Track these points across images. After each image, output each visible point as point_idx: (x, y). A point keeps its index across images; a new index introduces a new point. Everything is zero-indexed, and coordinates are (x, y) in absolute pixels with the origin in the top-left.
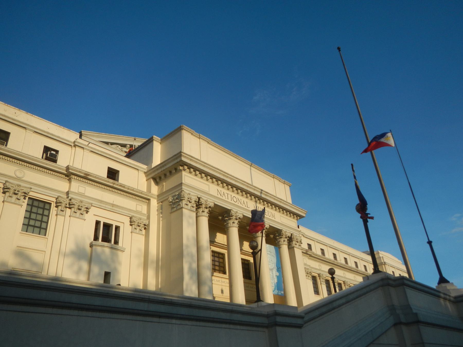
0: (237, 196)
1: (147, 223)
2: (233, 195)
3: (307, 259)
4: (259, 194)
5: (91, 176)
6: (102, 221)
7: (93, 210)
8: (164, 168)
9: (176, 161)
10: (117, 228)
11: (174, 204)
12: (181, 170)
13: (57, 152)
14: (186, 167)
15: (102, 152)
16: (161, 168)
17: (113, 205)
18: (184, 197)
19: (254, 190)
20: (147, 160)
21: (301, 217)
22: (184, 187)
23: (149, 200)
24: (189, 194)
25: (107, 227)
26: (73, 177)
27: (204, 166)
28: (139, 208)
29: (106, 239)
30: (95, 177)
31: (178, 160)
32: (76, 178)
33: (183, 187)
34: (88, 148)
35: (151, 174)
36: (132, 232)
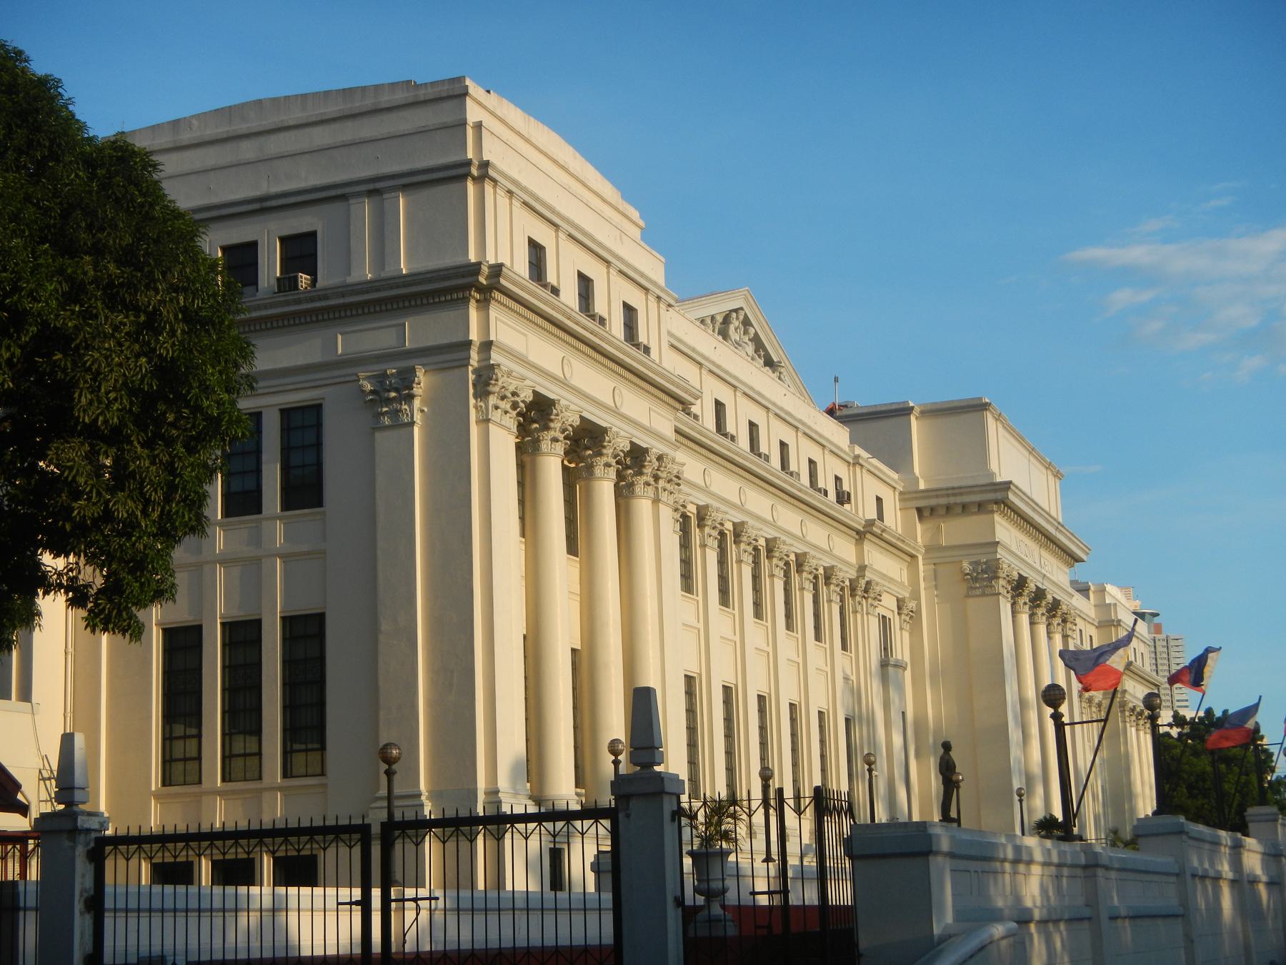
1: (912, 605)
4: (1052, 530)
8: (959, 500)
9: (992, 496)
11: (975, 580)
12: (992, 512)
15: (876, 467)
16: (948, 495)
17: (891, 580)
20: (897, 456)
21: (1077, 560)
22: (1001, 553)
23: (913, 557)
31: (999, 496)
33: (999, 550)
35: (916, 498)
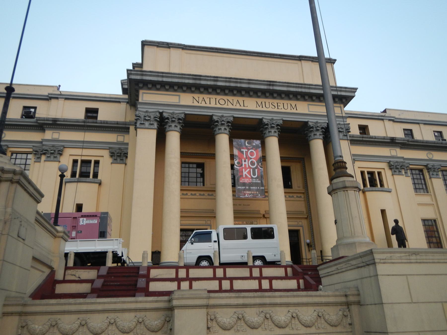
0: (226, 98)
2: (219, 97)
3: (398, 150)
5: (59, 121)
6: (79, 159)
7: (68, 152)
10: (97, 163)
13: (35, 108)
14: (141, 85)
18: (139, 117)
19: (249, 83)
24: (147, 112)
25: (86, 163)
26: (45, 126)
27: (163, 77)
28: (121, 139)
29: (84, 175)
30: (64, 121)
32: (47, 126)
34: (62, 96)
36: (112, 163)
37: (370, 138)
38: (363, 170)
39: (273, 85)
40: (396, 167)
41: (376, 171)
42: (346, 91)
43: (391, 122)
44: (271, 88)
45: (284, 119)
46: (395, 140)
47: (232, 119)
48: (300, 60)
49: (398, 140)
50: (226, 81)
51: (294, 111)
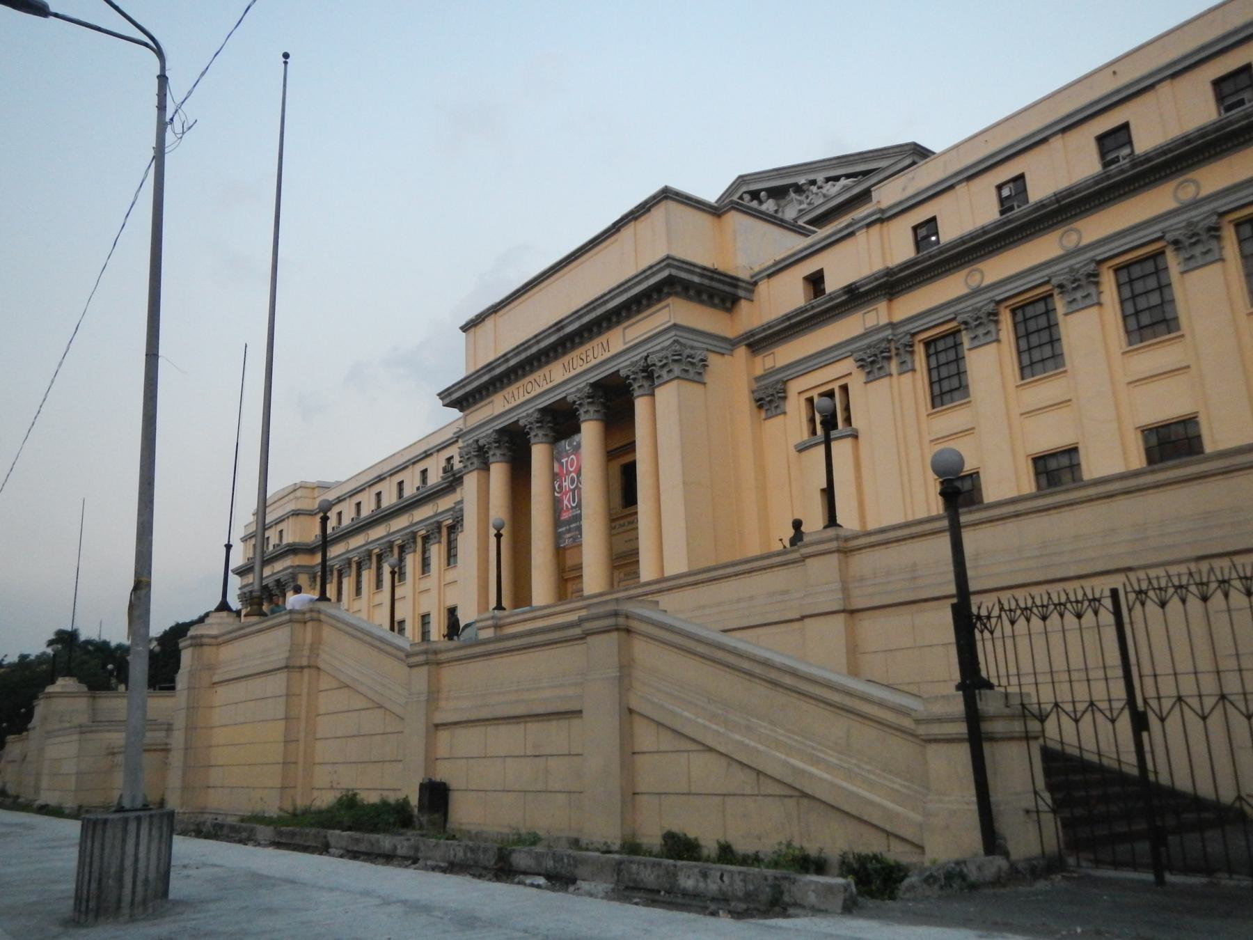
0: (530, 378)
3: (882, 306)
19: (538, 342)
37: (832, 299)
38: (808, 395)
39: (563, 328)
40: (876, 358)
41: (836, 386)
42: (654, 274)
43: (876, 228)
44: (562, 334)
45: (592, 381)
46: (858, 288)
47: (536, 415)
48: (618, 230)
49: (863, 286)
50: (516, 355)
51: (607, 355)
